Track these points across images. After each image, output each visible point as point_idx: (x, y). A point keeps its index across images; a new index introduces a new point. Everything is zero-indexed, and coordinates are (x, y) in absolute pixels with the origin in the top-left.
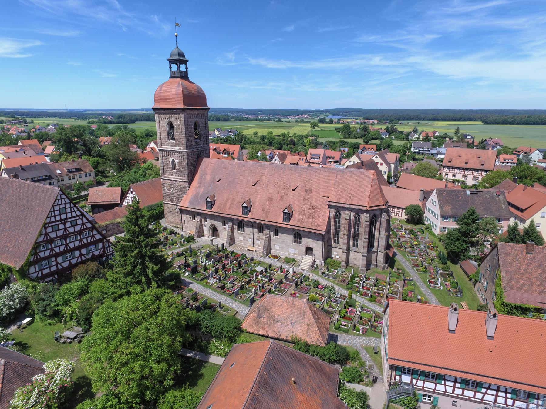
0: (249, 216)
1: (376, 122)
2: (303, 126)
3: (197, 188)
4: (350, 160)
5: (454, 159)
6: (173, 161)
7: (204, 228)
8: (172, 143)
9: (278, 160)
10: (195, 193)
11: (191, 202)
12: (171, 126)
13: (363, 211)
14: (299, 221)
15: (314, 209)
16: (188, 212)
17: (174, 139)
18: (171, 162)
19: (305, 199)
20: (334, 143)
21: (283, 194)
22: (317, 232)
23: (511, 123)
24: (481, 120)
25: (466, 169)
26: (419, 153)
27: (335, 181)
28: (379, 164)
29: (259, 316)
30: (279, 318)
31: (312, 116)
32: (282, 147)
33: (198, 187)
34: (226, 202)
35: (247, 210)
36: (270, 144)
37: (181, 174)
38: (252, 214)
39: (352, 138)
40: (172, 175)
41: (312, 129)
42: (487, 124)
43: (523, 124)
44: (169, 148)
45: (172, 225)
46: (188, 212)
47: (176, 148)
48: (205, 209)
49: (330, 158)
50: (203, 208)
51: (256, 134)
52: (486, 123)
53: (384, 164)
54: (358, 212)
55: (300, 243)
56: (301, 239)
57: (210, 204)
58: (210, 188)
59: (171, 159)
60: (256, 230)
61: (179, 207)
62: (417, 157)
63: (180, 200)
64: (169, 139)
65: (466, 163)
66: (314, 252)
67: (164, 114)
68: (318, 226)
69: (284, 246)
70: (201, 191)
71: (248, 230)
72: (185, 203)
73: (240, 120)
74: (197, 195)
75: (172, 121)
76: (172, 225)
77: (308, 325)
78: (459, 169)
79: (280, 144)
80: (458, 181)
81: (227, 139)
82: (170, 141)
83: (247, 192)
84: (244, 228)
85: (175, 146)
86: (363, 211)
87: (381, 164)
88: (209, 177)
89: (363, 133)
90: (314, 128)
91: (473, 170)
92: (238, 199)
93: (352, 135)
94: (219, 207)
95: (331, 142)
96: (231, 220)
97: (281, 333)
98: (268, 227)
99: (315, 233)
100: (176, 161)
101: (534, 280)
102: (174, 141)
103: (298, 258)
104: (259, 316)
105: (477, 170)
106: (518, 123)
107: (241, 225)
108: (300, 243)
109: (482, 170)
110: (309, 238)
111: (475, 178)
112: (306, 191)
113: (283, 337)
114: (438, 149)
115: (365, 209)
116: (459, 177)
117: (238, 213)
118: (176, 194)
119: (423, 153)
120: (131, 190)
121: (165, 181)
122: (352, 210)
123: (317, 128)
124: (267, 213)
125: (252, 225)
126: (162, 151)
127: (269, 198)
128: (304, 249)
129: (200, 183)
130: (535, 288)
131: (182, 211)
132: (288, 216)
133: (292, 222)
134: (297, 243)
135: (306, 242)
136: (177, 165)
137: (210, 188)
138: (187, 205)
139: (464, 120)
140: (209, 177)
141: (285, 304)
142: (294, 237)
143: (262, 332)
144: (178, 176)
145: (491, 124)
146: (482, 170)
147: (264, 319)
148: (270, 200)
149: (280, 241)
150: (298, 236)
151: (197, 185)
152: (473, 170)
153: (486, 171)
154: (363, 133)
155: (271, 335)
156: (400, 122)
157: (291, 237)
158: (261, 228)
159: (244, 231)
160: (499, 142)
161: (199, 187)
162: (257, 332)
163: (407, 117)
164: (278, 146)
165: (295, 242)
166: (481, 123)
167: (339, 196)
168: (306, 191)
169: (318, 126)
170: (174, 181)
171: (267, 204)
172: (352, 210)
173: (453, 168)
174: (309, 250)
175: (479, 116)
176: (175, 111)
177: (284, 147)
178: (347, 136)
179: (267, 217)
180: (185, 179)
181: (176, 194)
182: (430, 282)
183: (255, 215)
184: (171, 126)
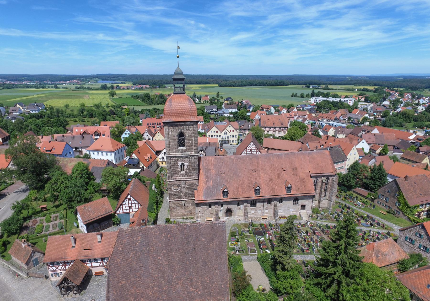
0: (261, 195)
1: (148, 87)
2: (95, 94)
3: (205, 183)
4: (211, 130)
5: (266, 122)
6: (182, 165)
7: (220, 212)
8: (182, 150)
9: (149, 135)
10: (205, 187)
11: (206, 195)
12: (181, 135)
13: (331, 176)
14: (296, 190)
15: (302, 180)
16: (205, 204)
17: (184, 146)
18: (180, 166)
19: (294, 175)
20: (149, 110)
21: (278, 174)
22: (311, 194)
23: (234, 86)
24: (216, 83)
25: (275, 128)
26: (210, 114)
27: (309, 160)
28: (232, 131)
29: (378, 257)
30: (386, 253)
31: (83, 81)
32: (106, 118)
33: (207, 181)
34: (238, 188)
35: (257, 191)
36: (91, 116)
37: (190, 174)
38: (262, 193)
39: (155, 104)
40: (180, 176)
41: (111, 97)
42: (222, 86)
43: (240, 86)
44: (179, 154)
45: (179, 217)
46: (205, 204)
47: (188, 154)
48: (222, 198)
49: (158, 124)
50: (220, 197)
51: (67, 106)
52: (220, 86)
53: (235, 130)
54: (328, 177)
55: (297, 204)
56: (298, 201)
57: (225, 193)
58: (218, 180)
59: (180, 164)
60: (266, 203)
61: (196, 202)
62: (212, 116)
63: (193, 195)
64: (178, 147)
65: (274, 124)
66: (306, 207)
67: (175, 126)
68: (309, 190)
69: (287, 209)
70: (211, 184)
71: (259, 205)
72: (200, 197)
73: (8, 88)
74: (208, 188)
75: (184, 131)
76: (179, 217)
77: (399, 250)
78: (270, 128)
79: (103, 115)
80: (271, 135)
81: (41, 114)
82: (179, 148)
83: (251, 177)
84: (255, 204)
85: (185, 152)
86: (331, 176)
87: (233, 131)
88: (213, 172)
89: (162, 100)
90: (113, 96)
91: (278, 127)
92: (246, 184)
93: (154, 102)
94: (233, 194)
95: (147, 110)
96: (246, 201)
97: (391, 261)
98: (276, 199)
99: (308, 196)
100: (185, 164)
101: (413, 193)
102: (184, 148)
103: (297, 214)
104: (378, 257)
105: (280, 128)
106: (237, 86)
107: (253, 203)
108: (297, 204)
109: (283, 127)
110: (304, 199)
111: (280, 132)
112: (293, 169)
113: (393, 262)
114: (223, 110)
115: (333, 174)
116: (271, 133)
117: (252, 195)
118: (184, 191)
119: (213, 114)
120: (129, 197)
121: (172, 182)
122: (325, 176)
123: (115, 97)
124: (273, 190)
125: (263, 201)
126: (171, 157)
127: (269, 179)
128: (300, 207)
129: (207, 177)
130: (415, 196)
131: (198, 205)
132: (289, 189)
133: (293, 192)
134: (295, 204)
135: (301, 202)
136: (186, 167)
137: (218, 180)
138: (203, 198)
139: (204, 84)
140: (213, 172)
141: (385, 244)
142: (294, 201)
143: (383, 265)
144: (188, 176)
145: (223, 86)
146: (283, 127)
147: (380, 257)
148: (271, 180)
149: (284, 206)
150: (296, 200)
151: (205, 180)
152: (278, 127)
153: (285, 128)
154: (162, 100)
155: (388, 264)
156: (166, 86)
157: (292, 202)
158: (269, 201)
159: (255, 206)
160: (249, 102)
161: (208, 181)
162: (381, 266)
163: (166, 82)
164: (103, 117)
165: (293, 204)
166: (217, 85)
167: (315, 169)
168: (293, 169)
169: (116, 94)
170: (182, 181)
171: (270, 183)
172: (325, 176)
173: (267, 127)
174: (303, 207)
175: (212, 80)
176: (189, 123)
177: (108, 117)
178: (150, 103)
179: (274, 193)
180: (194, 177)
181: (184, 191)
182: (356, 205)
183: (265, 193)
184: (181, 135)
